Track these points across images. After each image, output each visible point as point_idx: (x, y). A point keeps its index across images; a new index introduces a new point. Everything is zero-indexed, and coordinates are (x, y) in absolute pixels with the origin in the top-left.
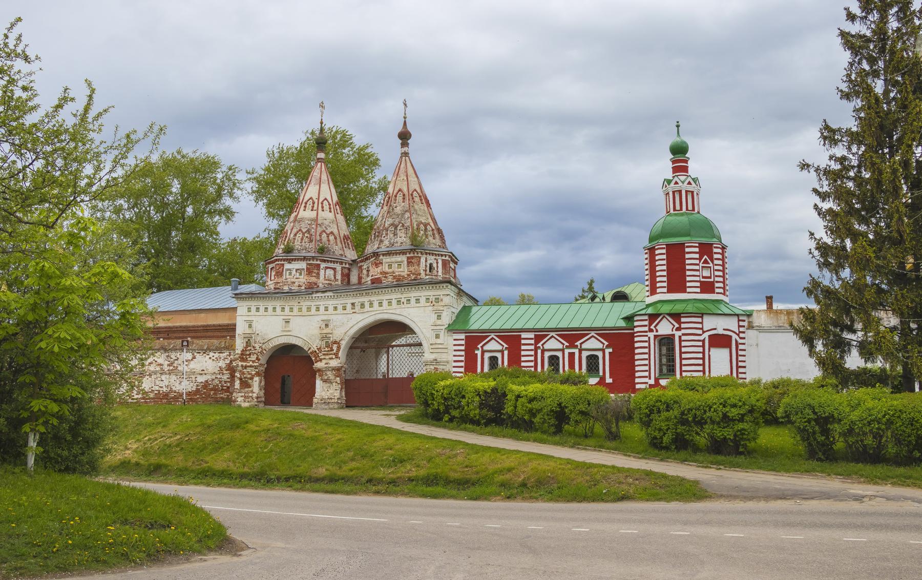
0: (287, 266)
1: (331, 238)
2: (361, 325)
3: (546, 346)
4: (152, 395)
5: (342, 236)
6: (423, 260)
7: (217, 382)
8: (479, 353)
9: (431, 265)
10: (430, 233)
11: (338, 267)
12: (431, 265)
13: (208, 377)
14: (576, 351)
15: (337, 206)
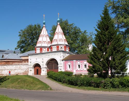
0: (37, 48)
1: (45, 42)
2: (48, 59)
3: (78, 63)
4: (17, 73)
5: (48, 42)
6: (60, 46)
7: (27, 71)
8: (67, 64)
9: (61, 47)
10: (62, 41)
11: (46, 48)
12: (61, 47)
13: (26, 70)
14: (82, 64)
15: (47, 36)
